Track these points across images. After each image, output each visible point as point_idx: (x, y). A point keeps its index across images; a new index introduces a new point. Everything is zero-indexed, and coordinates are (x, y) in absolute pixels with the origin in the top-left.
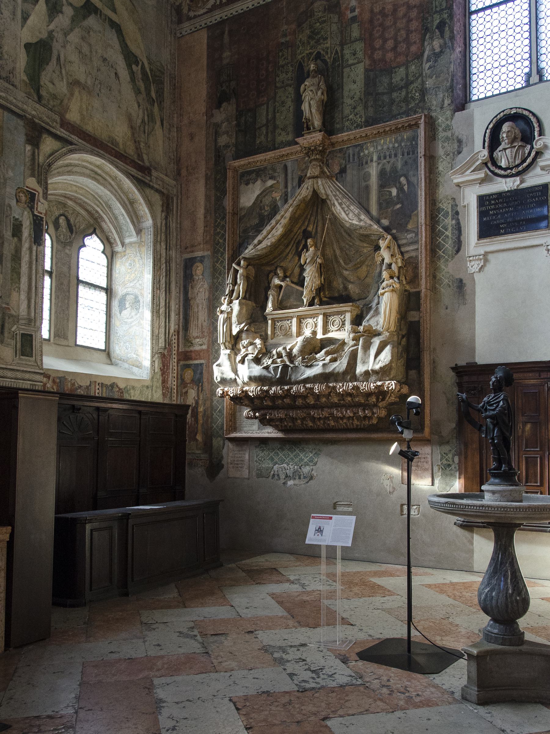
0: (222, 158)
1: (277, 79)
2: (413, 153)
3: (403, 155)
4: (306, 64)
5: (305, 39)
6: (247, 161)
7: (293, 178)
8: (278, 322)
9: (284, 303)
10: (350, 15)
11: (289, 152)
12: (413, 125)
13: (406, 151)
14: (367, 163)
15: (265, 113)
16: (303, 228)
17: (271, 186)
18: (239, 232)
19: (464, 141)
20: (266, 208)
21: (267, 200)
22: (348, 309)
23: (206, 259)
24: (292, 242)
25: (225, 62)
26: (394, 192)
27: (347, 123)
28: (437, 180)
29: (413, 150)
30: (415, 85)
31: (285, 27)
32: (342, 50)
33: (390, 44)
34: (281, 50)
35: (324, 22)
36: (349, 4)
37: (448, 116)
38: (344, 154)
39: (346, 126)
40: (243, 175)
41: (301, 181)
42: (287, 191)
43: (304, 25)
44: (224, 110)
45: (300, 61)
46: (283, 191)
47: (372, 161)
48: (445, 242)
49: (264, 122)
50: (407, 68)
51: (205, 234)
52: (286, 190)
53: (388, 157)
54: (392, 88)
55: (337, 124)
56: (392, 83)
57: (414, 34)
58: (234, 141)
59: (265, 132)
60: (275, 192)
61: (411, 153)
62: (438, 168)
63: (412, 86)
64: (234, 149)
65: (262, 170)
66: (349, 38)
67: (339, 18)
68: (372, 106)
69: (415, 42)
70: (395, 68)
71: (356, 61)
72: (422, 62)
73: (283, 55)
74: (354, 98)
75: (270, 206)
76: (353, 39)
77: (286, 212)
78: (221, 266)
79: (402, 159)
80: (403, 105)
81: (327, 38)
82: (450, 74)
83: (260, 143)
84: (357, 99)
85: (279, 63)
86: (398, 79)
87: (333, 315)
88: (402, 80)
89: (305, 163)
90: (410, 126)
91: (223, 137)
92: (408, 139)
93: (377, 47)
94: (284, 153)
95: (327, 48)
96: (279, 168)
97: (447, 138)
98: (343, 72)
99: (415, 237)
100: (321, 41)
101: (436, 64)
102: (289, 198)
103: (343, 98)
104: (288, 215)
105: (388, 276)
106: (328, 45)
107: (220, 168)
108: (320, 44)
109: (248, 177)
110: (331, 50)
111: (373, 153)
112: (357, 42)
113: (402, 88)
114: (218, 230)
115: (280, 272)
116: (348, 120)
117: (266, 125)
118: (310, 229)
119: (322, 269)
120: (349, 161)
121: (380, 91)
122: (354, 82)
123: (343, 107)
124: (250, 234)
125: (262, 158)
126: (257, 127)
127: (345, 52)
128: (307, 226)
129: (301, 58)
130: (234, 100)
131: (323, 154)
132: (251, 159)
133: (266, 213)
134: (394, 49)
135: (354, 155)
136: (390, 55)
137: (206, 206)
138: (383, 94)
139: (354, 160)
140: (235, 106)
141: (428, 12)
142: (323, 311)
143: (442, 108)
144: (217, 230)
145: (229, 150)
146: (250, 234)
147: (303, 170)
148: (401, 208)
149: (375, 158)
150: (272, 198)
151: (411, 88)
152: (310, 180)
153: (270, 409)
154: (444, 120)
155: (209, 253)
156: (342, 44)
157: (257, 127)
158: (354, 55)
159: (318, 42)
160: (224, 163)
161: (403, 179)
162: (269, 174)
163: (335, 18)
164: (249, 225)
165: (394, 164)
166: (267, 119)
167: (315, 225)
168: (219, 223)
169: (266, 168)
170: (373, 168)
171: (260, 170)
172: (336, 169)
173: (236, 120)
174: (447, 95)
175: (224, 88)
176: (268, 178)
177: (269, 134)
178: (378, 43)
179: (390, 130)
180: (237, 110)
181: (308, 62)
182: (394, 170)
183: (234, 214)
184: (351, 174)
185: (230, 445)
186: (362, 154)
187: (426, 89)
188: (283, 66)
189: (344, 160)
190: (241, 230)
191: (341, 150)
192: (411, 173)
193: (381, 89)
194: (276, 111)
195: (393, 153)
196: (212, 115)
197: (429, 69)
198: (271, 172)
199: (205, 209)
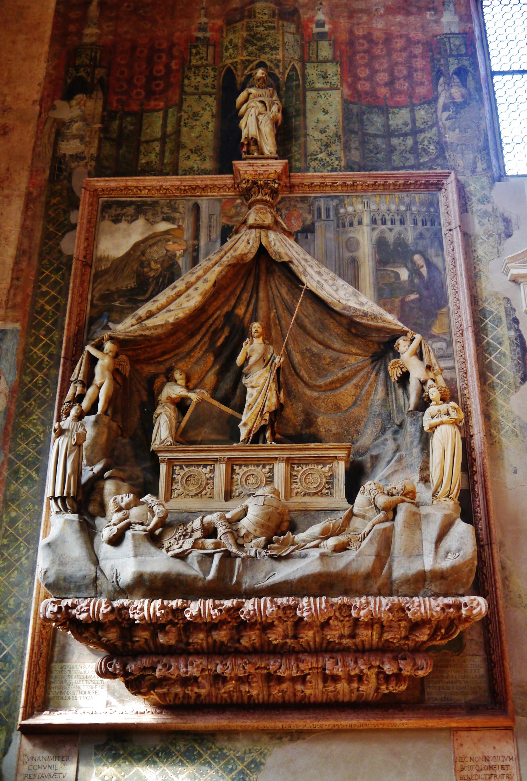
0: (65, 174)
1: (186, 82)
2: (433, 224)
3: (415, 223)
4: (239, 73)
5: (239, 42)
6: (123, 184)
7: (210, 226)
8: (181, 468)
9: (192, 434)
10: (316, 30)
11: (209, 182)
12: (432, 184)
13: (419, 219)
14: (351, 225)
15: (161, 122)
16: (226, 309)
17: (167, 232)
18: (93, 297)
19: (514, 221)
20: (153, 265)
21: (157, 253)
22: (342, 454)
23: (9, 337)
24: (204, 330)
25: (87, 40)
26: (404, 274)
27: (313, 164)
28: (475, 268)
29: (433, 219)
30: (428, 135)
31: (204, 20)
32: (304, 68)
33: (382, 77)
34: (195, 47)
35: (274, 28)
36: (314, 17)
37: (485, 184)
38: (310, 206)
39: (312, 166)
40: (107, 206)
41: (227, 233)
42: (198, 245)
43: (239, 25)
44: (78, 104)
45: (229, 69)
46: (191, 242)
47: (360, 223)
48: (500, 362)
49: (158, 134)
50: (412, 111)
51: (12, 292)
52: (196, 242)
53: (389, 223)
54: (389, 133)
55: (296, 161)
56: (389, 126)
57: (420, 74)
58: (93, 151)
59: (157, 149)
60: (174, 243)
61: (429, 223)
62: (475, 251)
63: (423, 135)
64: (93, 163)
65: (150, 205)
66: (314, 56)
67: (298, 28)
68: (356, 148)
69: (422, 83)
70: (392, 107)
71: (328, 86)
72: (436, 109)
73: (198, 53)
74: (325, 132)
75: (162, 263)
76: (320, 58)
77: (205, 273)
78: (44, 353)
79: (414, 229)
80: (411, 156)
81: (276, 48)
82: (482, 132)
83: (147, 163)
84: (331, 134)
85: (190, 61)
86: (400, 122)
87: (307, 464)
88: (406, 124)
89: (236, 207)
90: (428, 185)
91: (72, 142)
92: (422, 204)
93: (362, 76)
94: (199, 183)
95: (279, 61)
96: (184, 206)
97: (486, 213)
98: (305, 97)
99: (447, 348)
100: (267, 50)
101: (458, 116)
102: (201, 256)
103: (306, 128)
104: (212, 276)
105: (439, 396)
106: (280, 57)
107: (59, 187)
108: (265, 53)
109: (117, 210)
110: (284, 65)
111: (362, 212)
112: (328, 64)
113: (406, 135)
114: (44, 289)
115: (177, 375)
116: (316, 159)
117: (163, 140)
118: (240, 311)
119: (282, 379)
120: (319, 216)
121: (370, 131)
122: (326, 112)
123: (305, 142)
124: (117, 304)
125: (155, 183)
126: (143, 139)
127: (306, 71)
128: (234, 307)
129: (232, 64)
130: (100, 95)
131: (279, 194)
132: (131, 181)
133: (152, 274)
134: (391, 83)
135: (328, 210)
136: (383, 91)
137: (20, 243)
138: (375, 136)
139: (328, 216)
140: (100, 103)
141: (440, 53)
142: (287, 454)
143: (474, 171)
144: (40, 287)
145: (82, 163)
146: (117, 304)
147: (232, 217)
148: (419, 300)
149: (366, 220)
150: (167, 251)
151: (422, 137)
152: (253, 230)
153: (164, 655)
154: (478, 188)
155: (18, 326)
156: (303, 61)
157: (143, 139)
158: (324, 78)
159: (261, 49)
160: (70, 181)
161: (417, 258)
162: (162, 213)
163: (292, 28)
164: (113, 288)
165: (400, 234)
166: (164, 134)
167: (251, 307)
168: (48, 277)
169: (157, 202)
170: (363, 233)
171: (145, 203)
172: (296, 226)
173: (102, 122)
174: (479, 157)
175: (82, 73)
176: (158, 219)
177: (167, 154)
178: (363, 72)
179: (394, 184)
180: (104, 109)
181: (244, 70)
182: (400, 242)
183: (87, 264)
184: (324, 234)
185: (27, 746)
186: (342, 211)
187: (446, 143)
188: (198, 67)
189: (309, 213)
190: (97, 295)
191: (303, 200)
192: (431, 252)
193: (371, 130)
194: (182, 123)
195: (397, 218)
196: (54, 108)
197: (447, 119)
198: (165, 210)
199: (18, 249)
